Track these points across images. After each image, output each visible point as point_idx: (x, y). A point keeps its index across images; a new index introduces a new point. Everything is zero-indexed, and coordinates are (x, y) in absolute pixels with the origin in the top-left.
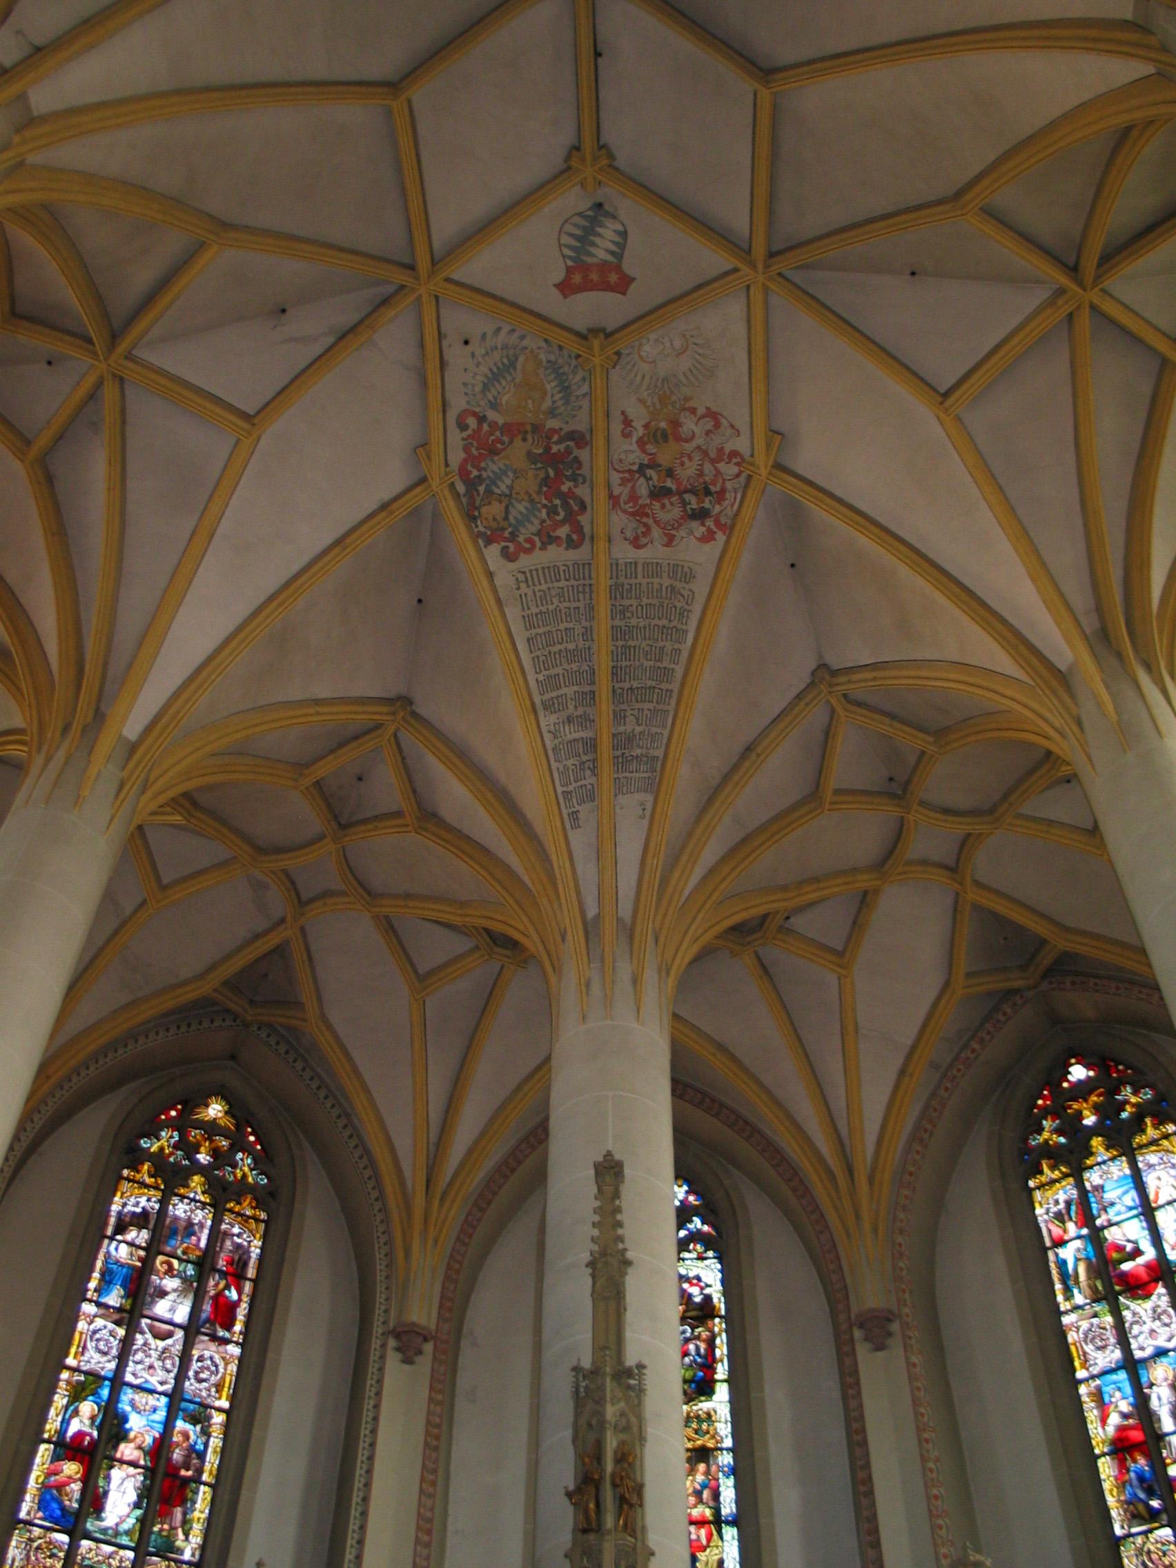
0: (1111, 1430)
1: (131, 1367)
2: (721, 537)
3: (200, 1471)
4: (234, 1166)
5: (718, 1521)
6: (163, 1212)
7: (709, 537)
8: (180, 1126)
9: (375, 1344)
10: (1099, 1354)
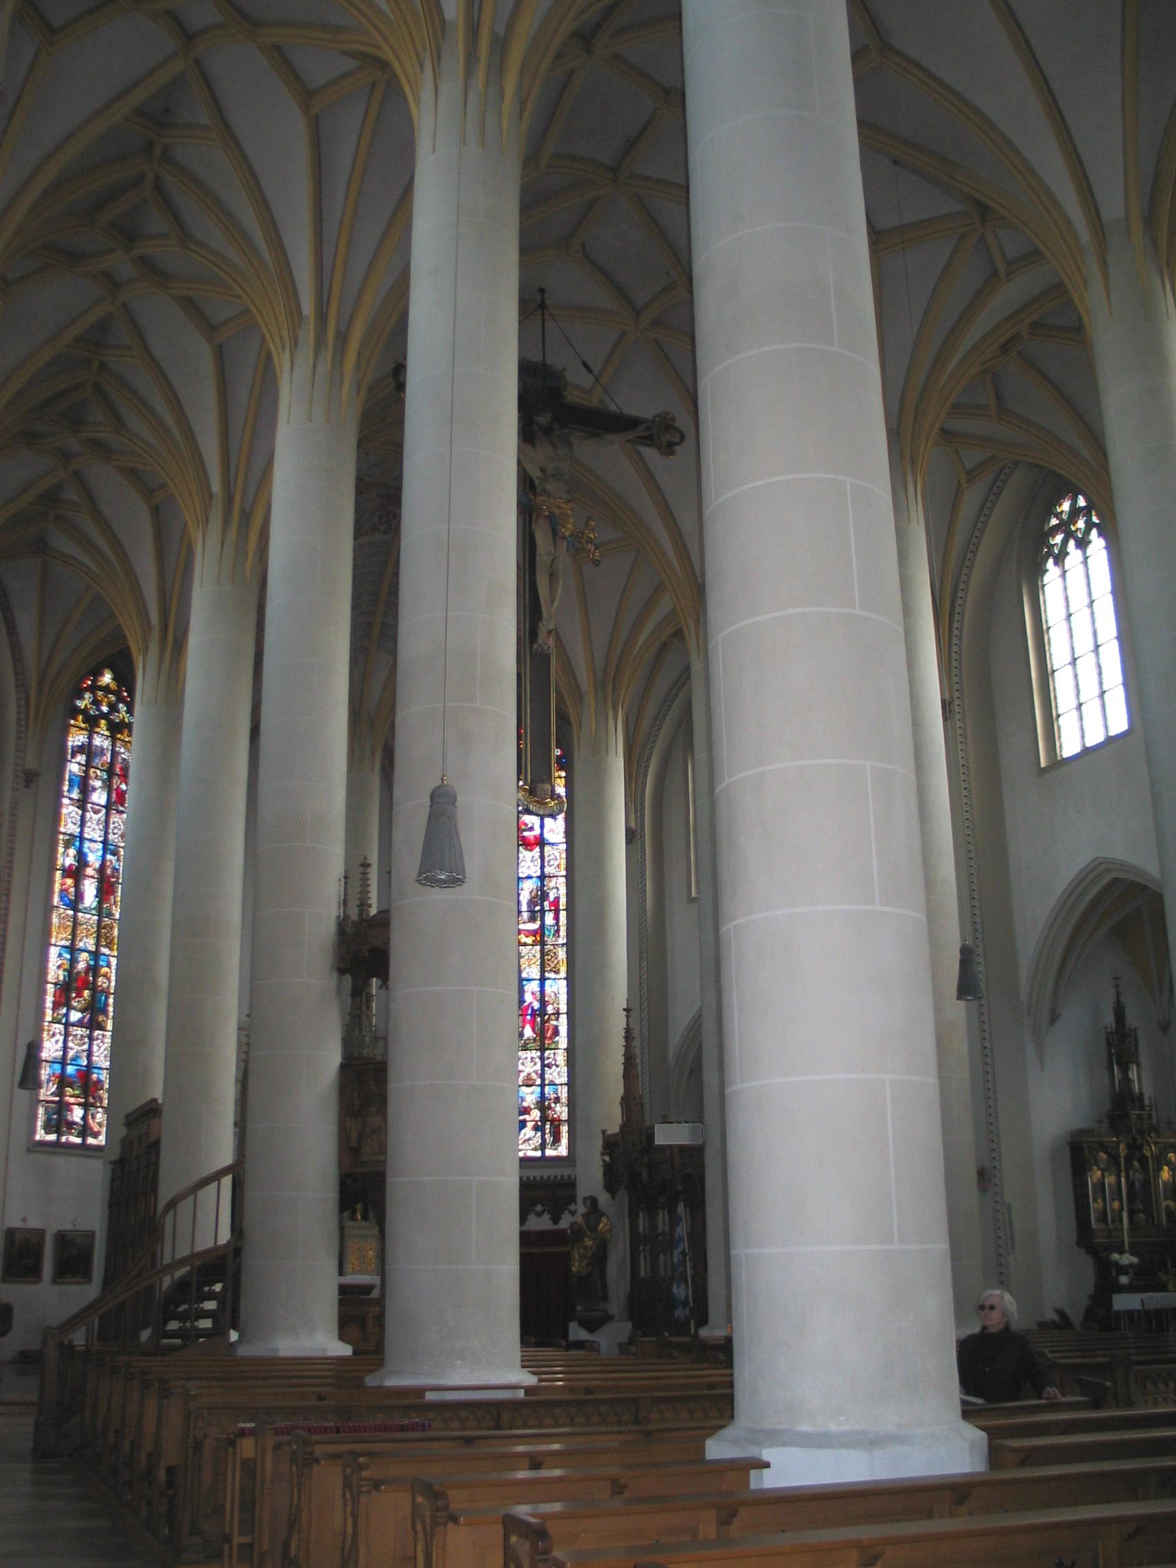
1: (86, 830)
4: (118, 712)
6: (90, 743)
8: (93, 689)
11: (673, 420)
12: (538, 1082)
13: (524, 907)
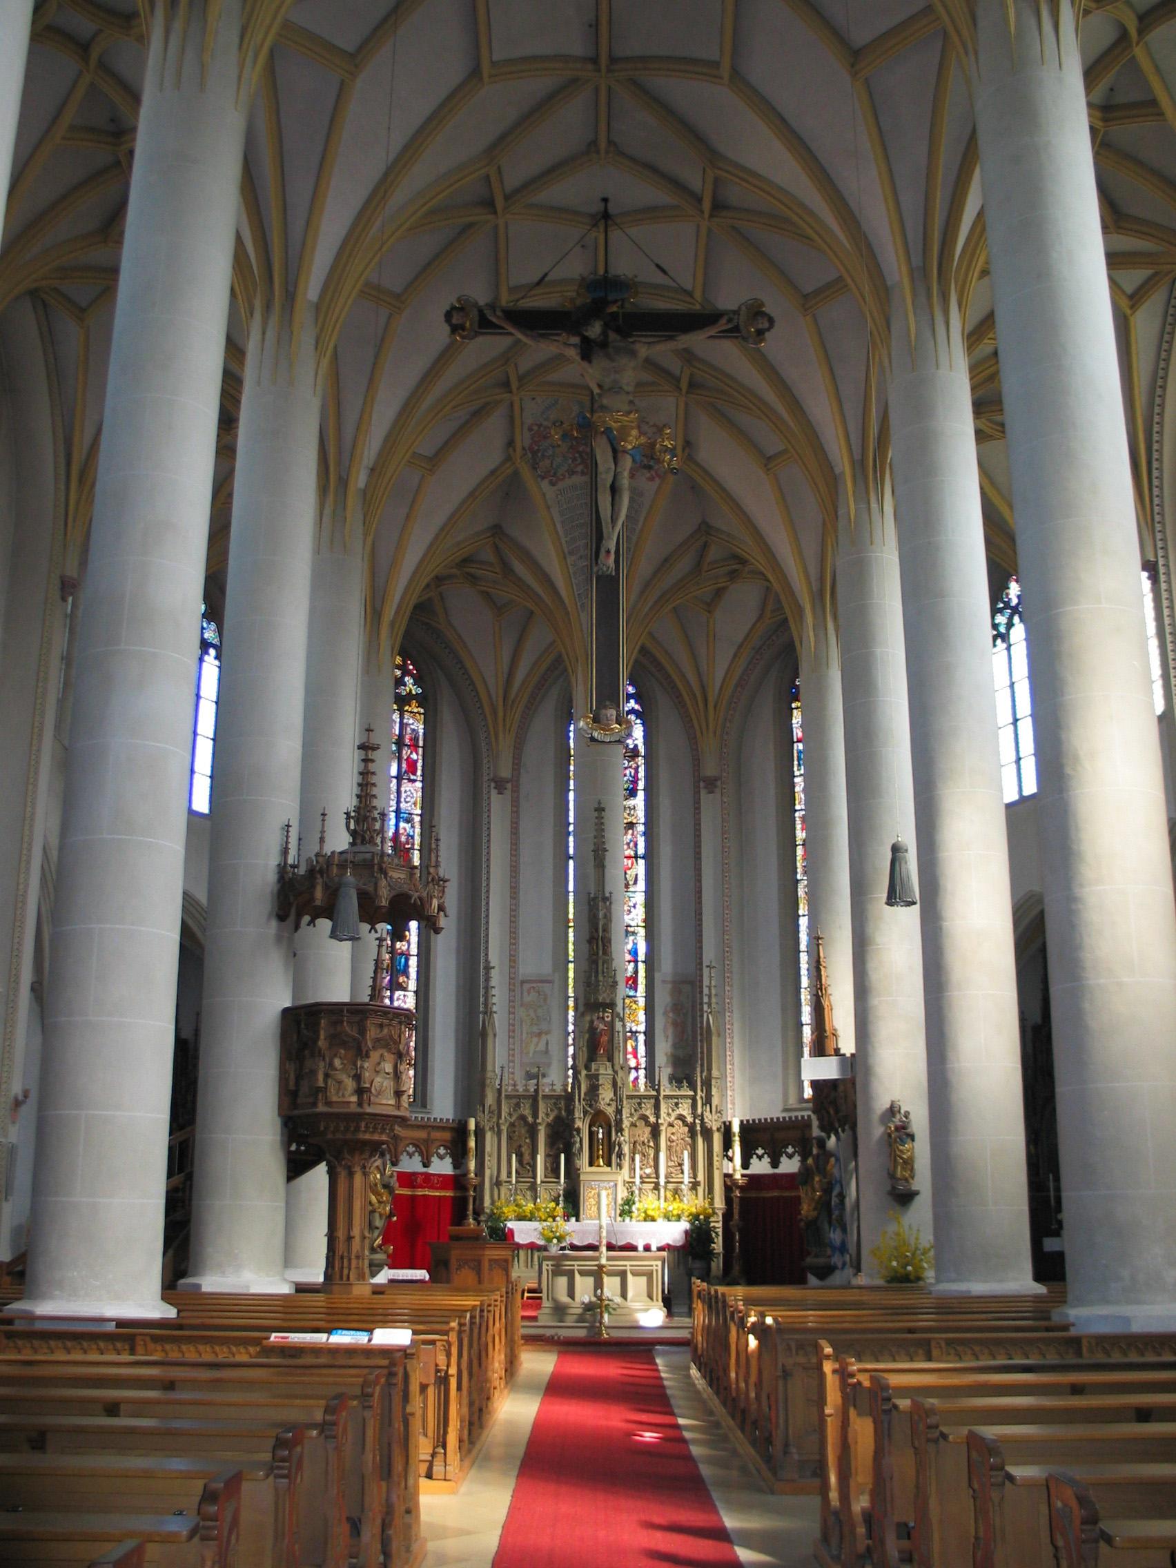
2: (657, 481)
3: (413, 844)
4: (405, 685)
5: (636, 857)
7: (651, 479)
9: (485, 785)
11: (762, 305)
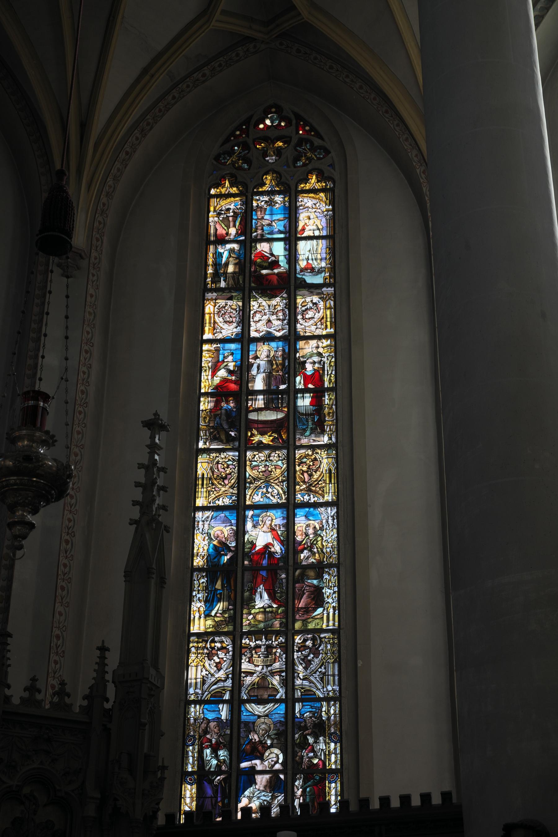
0: (217, 380)
10: (225, 326)
12: (281, 694)
13: (259, 384)
